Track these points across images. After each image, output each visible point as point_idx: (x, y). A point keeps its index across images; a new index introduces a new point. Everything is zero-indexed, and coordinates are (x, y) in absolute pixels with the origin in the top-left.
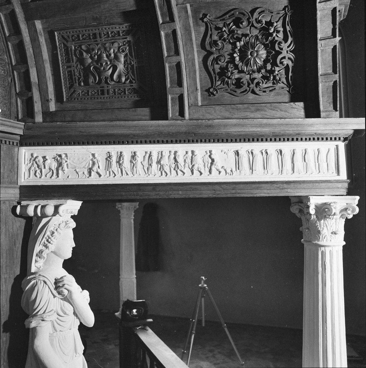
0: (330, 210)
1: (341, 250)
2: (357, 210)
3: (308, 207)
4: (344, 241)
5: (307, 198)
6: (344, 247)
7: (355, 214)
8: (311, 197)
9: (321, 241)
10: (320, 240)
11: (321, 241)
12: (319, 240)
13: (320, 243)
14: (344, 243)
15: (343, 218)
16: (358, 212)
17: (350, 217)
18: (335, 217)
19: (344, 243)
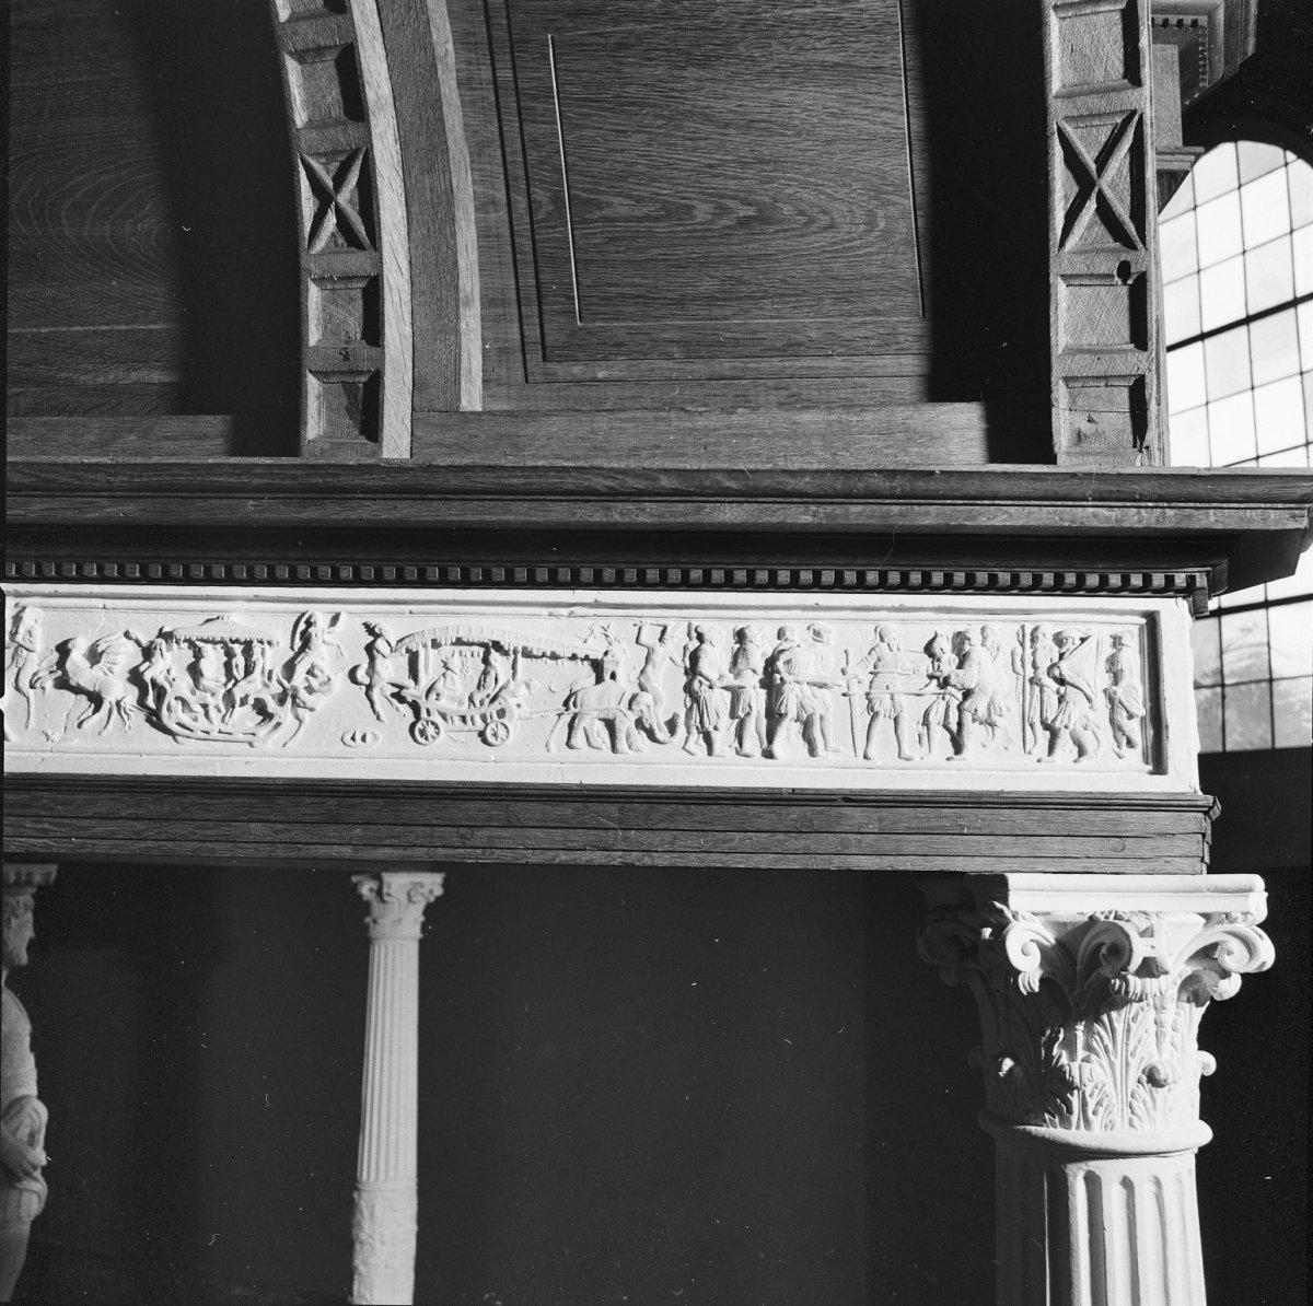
0: (1119, 950)
1: (1190, 1170)
2: (1266, 954)
3: (1001, 926)
4: (1202, 1117)
5: (997, 886)
6: (1204, 1156)
7: (1252, 968)
8: (1014, 880)
9: (1078, 1127)
10: (1074, 1118)
11: (1078, 1127)
12: (1066, 1123)
13: (1074, 1135)
14: (1205, 1134)
15: (1196, 999)
16: (1269, 965)
17: (1230, 988)
18: (1151, 985)
19: (1205, 1134)
